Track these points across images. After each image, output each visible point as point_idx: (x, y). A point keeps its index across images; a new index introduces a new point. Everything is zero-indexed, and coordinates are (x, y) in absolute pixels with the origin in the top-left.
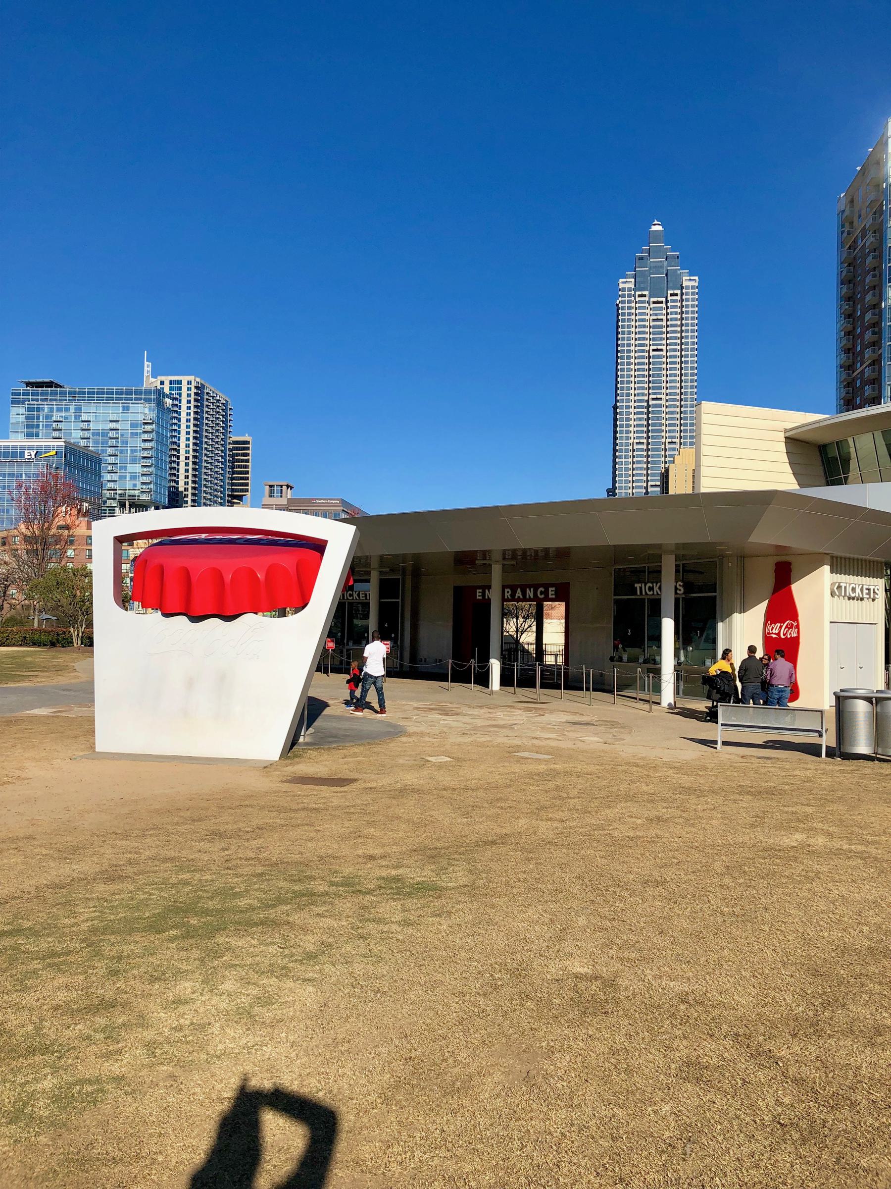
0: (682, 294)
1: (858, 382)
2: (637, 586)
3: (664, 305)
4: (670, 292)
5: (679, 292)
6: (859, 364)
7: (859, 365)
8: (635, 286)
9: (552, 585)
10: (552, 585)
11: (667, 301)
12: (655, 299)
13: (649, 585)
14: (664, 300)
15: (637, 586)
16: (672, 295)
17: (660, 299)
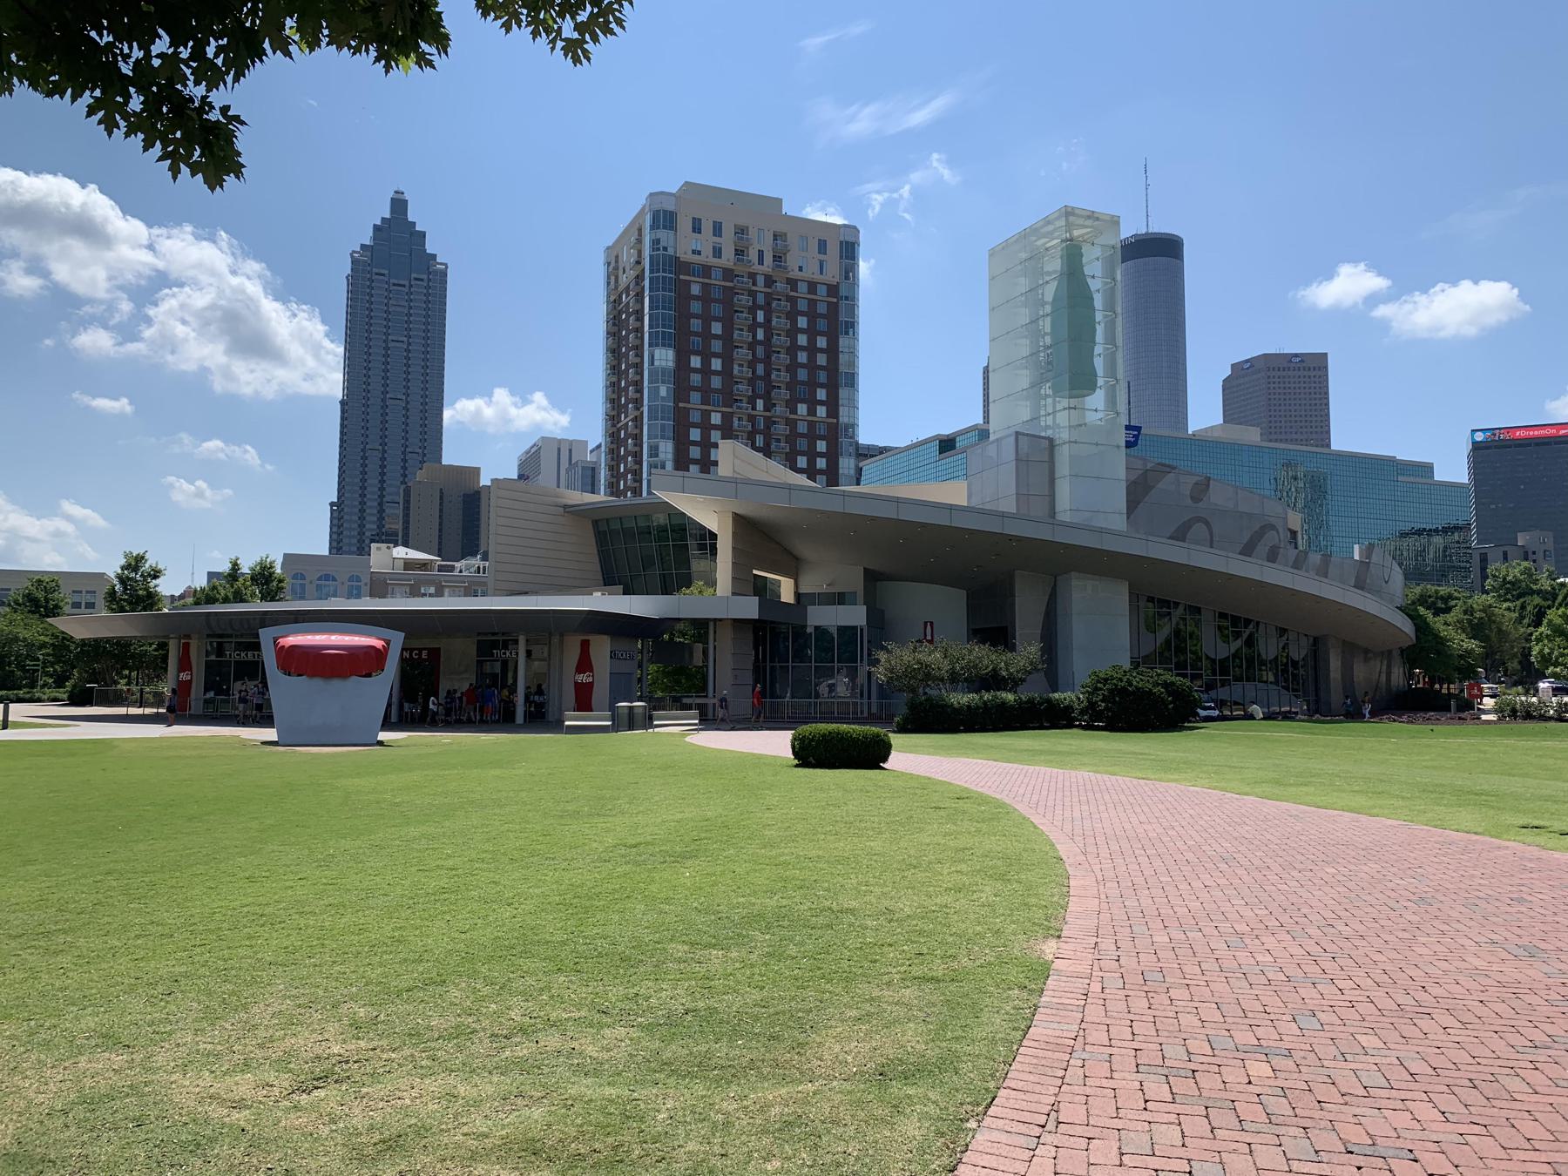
0: (429, 280)
1: (623, 432)
2: (495, 651)
3: (406, 290)
4: (414, 275)
5: (424, 277)
6: (623, 415)
7: (623, 415)
8: (372, 260)
9: (425, 649)
10: (425, 649)
11: (411, 286)
12: (396, 282)
13: (503, 651)
14: (407, 283)
15: (495, 651)
16: (416, 279)
17: (402, 282)
